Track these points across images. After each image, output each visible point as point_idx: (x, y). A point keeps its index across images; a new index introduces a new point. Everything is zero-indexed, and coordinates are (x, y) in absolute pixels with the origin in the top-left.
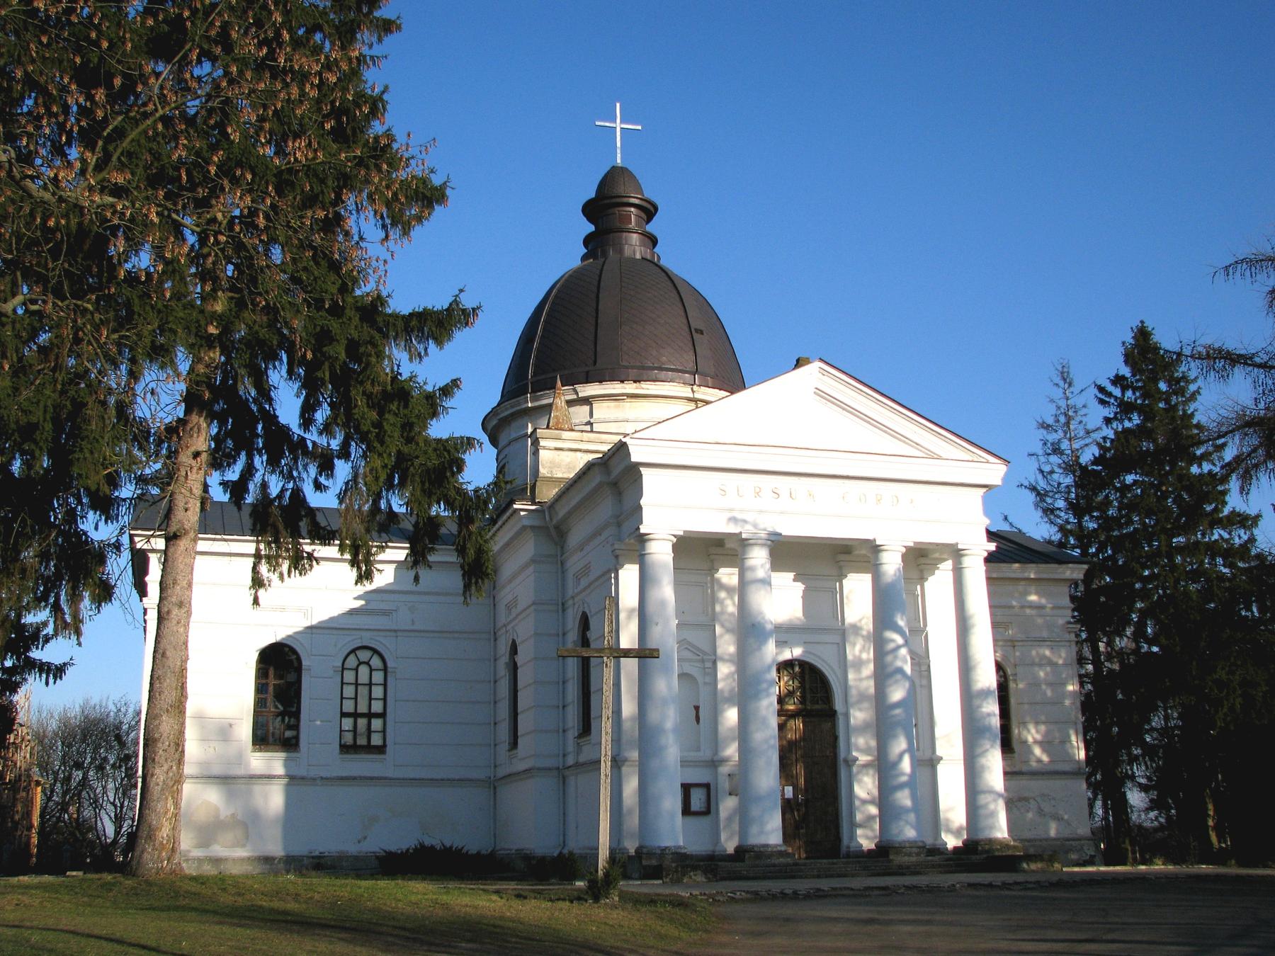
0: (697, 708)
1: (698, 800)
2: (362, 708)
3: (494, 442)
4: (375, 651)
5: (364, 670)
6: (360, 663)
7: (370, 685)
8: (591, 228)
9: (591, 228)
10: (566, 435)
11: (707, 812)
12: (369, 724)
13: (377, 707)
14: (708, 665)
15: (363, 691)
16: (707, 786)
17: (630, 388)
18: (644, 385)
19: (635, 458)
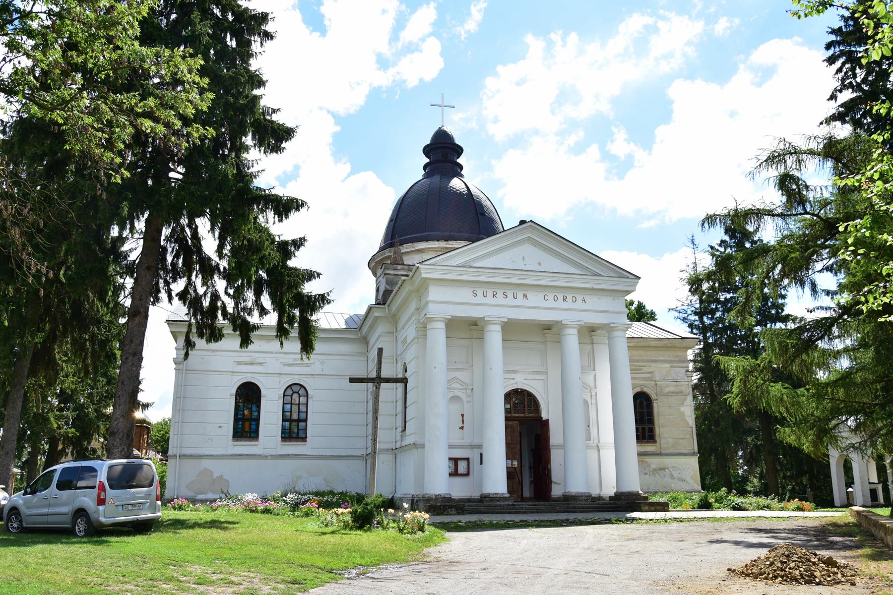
0: (463, 415)
1: (458, 468)
2: (295, 417)
3: (375, 274)
4: (302, 386)
5: (295, 396)
6: (294, 392)
7: (299, 404)
8: (428, 160)
9: (428, 160)
10: (399, 267)
11: (468, 474)
12: (298, 426)
13: (303, 416)
14: (469, 391)
15: (295, 408)
16: (468, 459)
17: (442, 244)
18: (450, 242)
19: (424, 275)
